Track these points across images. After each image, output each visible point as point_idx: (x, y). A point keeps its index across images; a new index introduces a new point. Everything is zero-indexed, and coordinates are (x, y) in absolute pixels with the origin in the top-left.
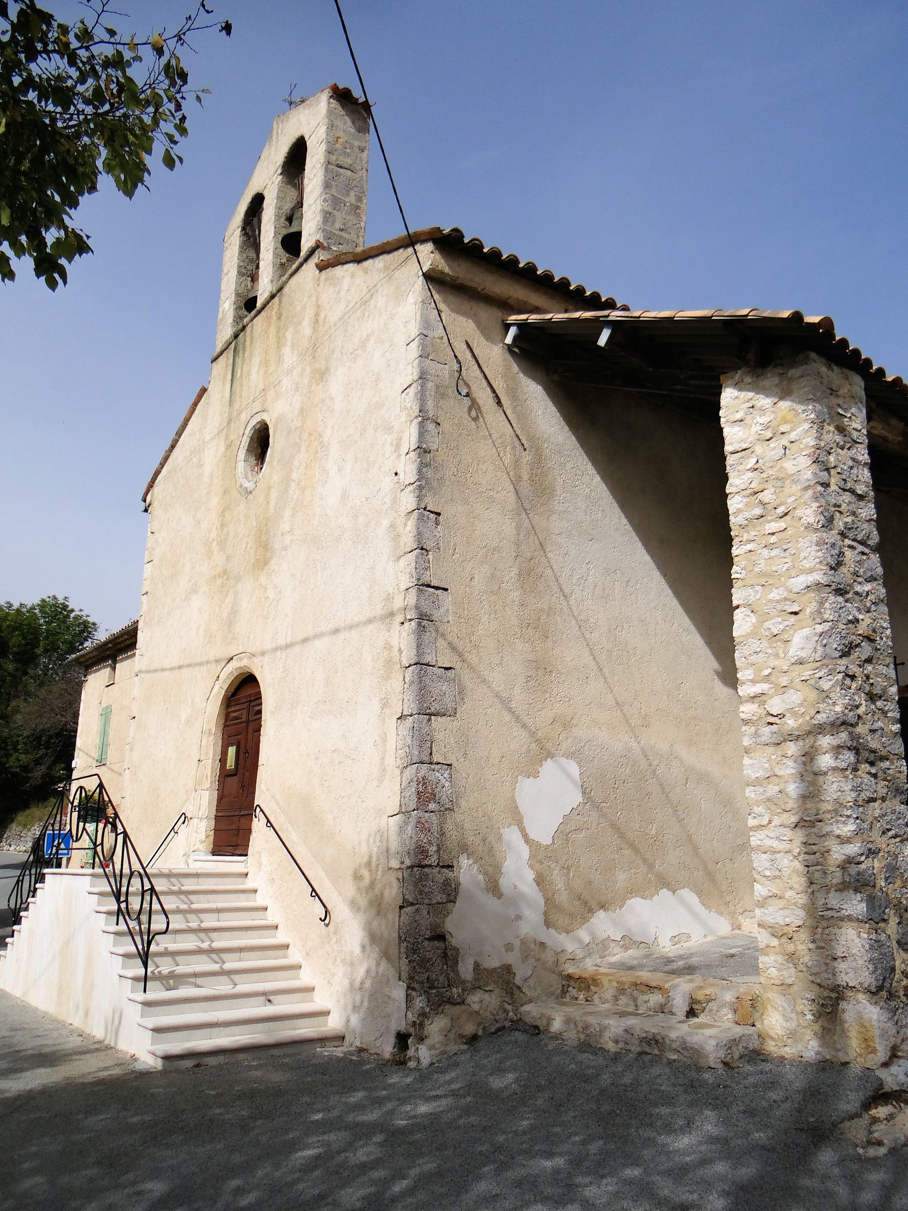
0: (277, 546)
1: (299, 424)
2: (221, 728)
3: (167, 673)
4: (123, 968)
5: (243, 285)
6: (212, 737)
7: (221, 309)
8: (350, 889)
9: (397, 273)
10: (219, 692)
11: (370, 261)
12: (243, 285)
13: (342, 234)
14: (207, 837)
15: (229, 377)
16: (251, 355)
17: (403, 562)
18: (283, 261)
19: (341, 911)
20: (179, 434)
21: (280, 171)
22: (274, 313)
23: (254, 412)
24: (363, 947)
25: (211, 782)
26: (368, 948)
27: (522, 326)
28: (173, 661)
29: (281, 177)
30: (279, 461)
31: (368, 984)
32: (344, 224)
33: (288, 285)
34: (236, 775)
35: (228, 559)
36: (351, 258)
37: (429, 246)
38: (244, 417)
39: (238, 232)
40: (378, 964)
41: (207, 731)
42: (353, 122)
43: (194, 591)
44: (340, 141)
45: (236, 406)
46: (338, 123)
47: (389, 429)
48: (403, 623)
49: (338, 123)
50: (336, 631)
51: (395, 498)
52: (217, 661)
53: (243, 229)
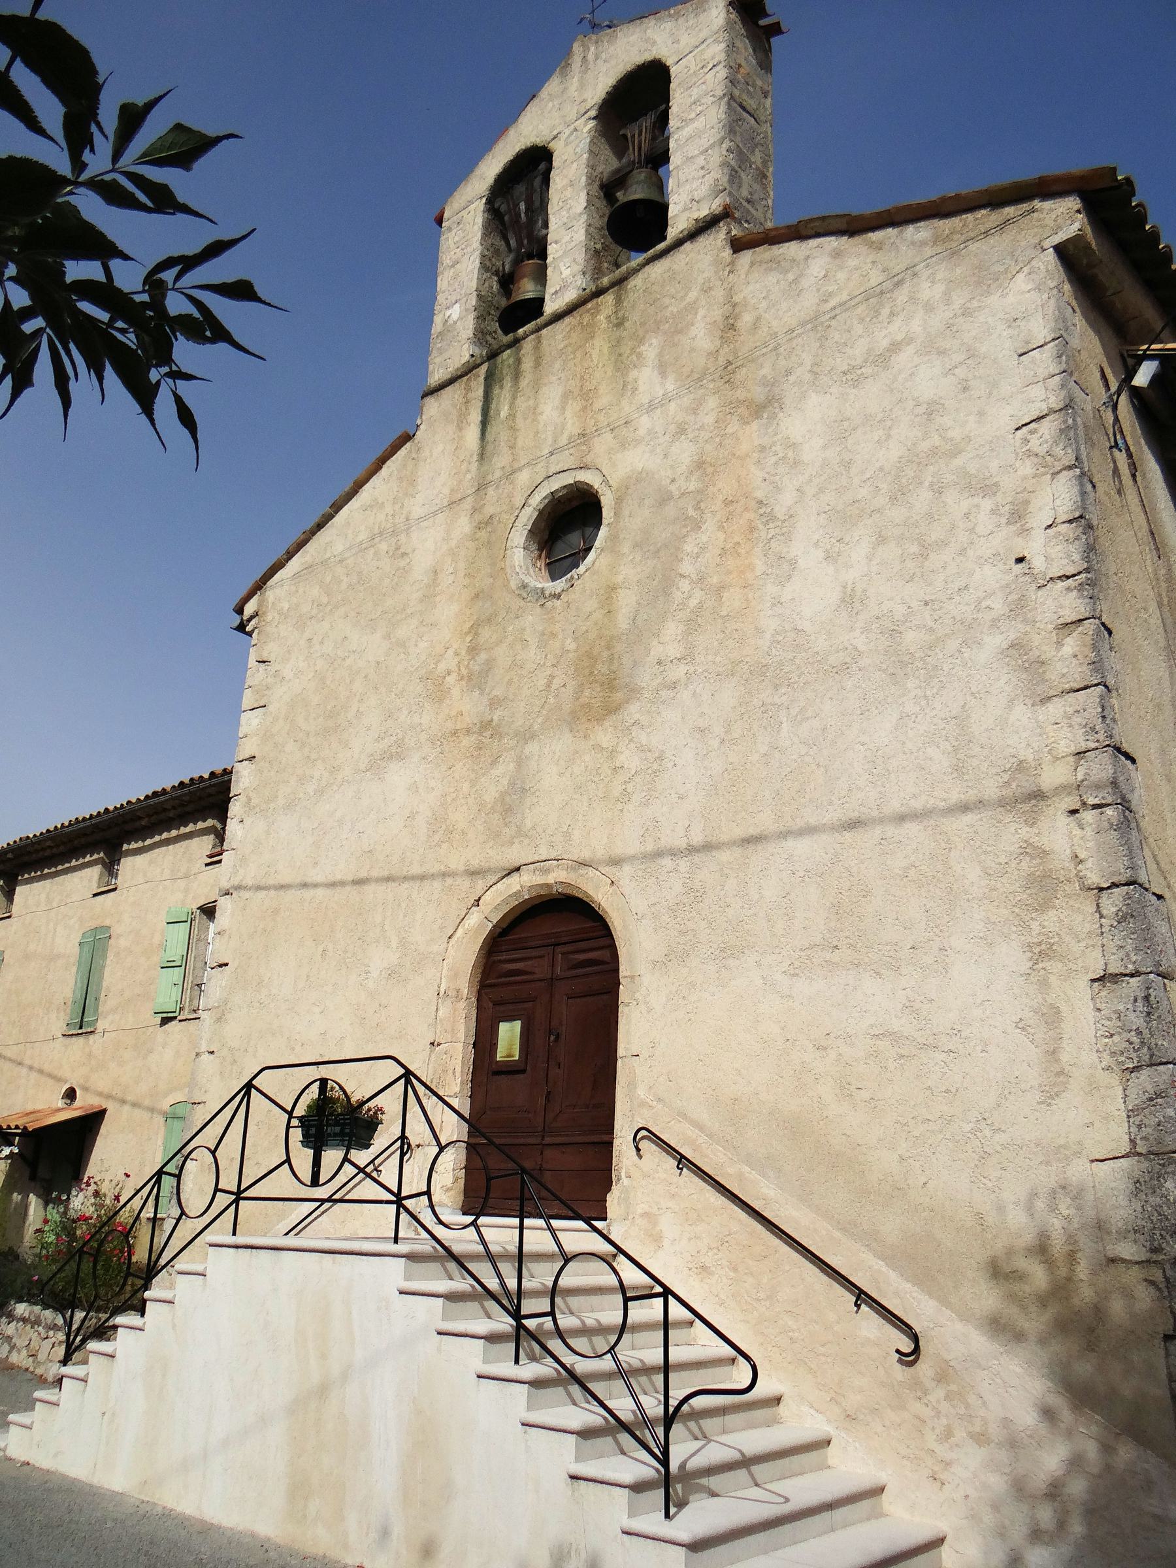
0: (646, 678)
1: (693, 485)
2: (475, 989)
3: (320, 892)
4: (578, 1459)
5: (486, 285)
6: (462, 1005)
7: (438, 320)
8: (988, 1298)
9: (973, 247)
10: (481, 926)
11: (890, 231)
12: (486, 285)
13: (749, 207)
14: (456, 1181)
15: (475, 416)
16: (537, 385)
17: (1056, 709)
18: (599, 246)
19: (952, 1333)
20: (337, 507)
21: (593, 113)
22: (601, 317)
23: (553, 470)
24: (1048, 1414)
25: (462, 1083)
26: (1066, 1415)
27: (1165, 359)
28: (344, 870)
29: (592, 123)
30: (636, 545)
31: (1077, 1488)
32: (751, 194)
33: (641, 275)
34: (523, 1071)
35: (494, 703)
36: (844, 227)
37: (1072, 203)
38: (524, 478)
39: (480, 205)
40: (1107, 1449)
41: (452, 993)
42: (754, 50)
43: (396, 753)
44: (742, 70)
45: (501, 460)
46: (738, 43)
47: (988, 489)
48: (1074, 812)
49: (738, 43)
50: (853, 825)
51: (1022, 598)
52: (473, 873)
53: (489, 202)
